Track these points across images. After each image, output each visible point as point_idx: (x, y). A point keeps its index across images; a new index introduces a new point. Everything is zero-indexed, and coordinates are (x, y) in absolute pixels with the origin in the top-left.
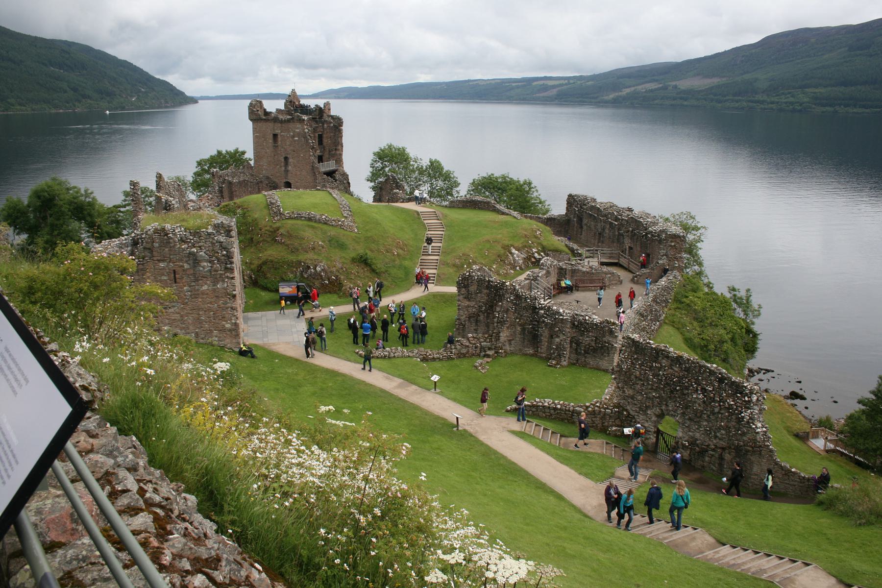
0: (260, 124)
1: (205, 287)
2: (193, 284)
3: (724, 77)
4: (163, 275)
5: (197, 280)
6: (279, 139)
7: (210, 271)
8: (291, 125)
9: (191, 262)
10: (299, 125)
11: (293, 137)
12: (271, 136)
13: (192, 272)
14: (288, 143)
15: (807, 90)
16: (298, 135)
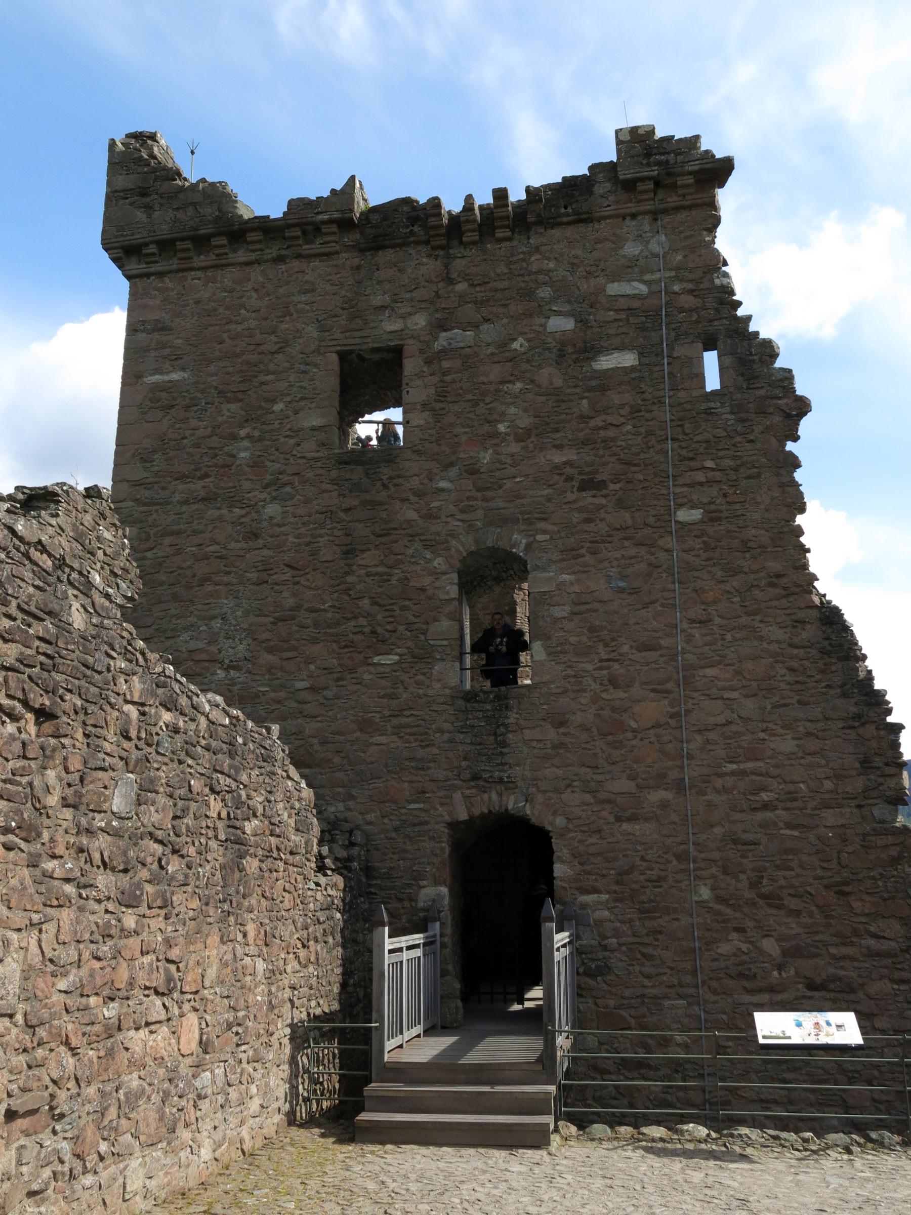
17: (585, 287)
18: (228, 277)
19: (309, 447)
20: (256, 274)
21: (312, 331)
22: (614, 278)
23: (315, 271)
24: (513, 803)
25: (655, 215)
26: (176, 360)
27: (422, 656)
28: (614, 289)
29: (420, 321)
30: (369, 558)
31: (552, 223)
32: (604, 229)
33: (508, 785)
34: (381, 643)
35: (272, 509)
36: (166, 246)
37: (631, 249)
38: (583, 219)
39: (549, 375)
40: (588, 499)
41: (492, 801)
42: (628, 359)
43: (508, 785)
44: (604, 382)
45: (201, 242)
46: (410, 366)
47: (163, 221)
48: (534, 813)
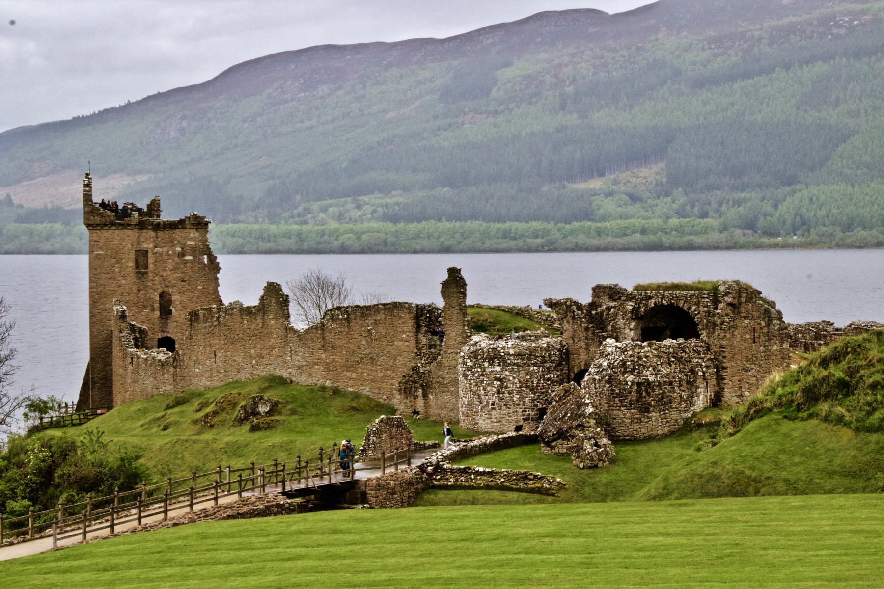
0: (106, 234)
1: (775, 348)
2: (767, 343)
3: (140, 172)
4: (746, 333)
5: (769, 340)
6: (151, 260)
7: (779, 330)
8: (178, 234)
9: (766, 319)
10: (193, 233)
11: (182, 255)
12: (132, 255)
13: (765, 330)
14: (170, 266)
15: (366, 198)
16: (193, 250)
17: (184, 242)
18: (111, 231)
19: (130, 270)
20: (117, 231)
21: (129, 246)
22: (189, 240)
23: (129, 232)
24: (169, 335)
25: (197, 229)
26: (101, 248)
27: (153, 310)
28: (189, 243)
29: (151, 246)
30: (142, 292)
31: (175, 228)
32: (187, 231)
33: (168, 332)
34: (145, 307)
35: (123, 281)
36: (97, 225)
37: (192, 235)
38: (184, 228)
39: (176, 259)
40: (183, 283)
41: (166, 334)
42: (190, 258)
43: (168, 332)
44: (186, 262)
45: (105, 225)
46: (150, 255)
47: (98, 220)
48: (173, 337)
